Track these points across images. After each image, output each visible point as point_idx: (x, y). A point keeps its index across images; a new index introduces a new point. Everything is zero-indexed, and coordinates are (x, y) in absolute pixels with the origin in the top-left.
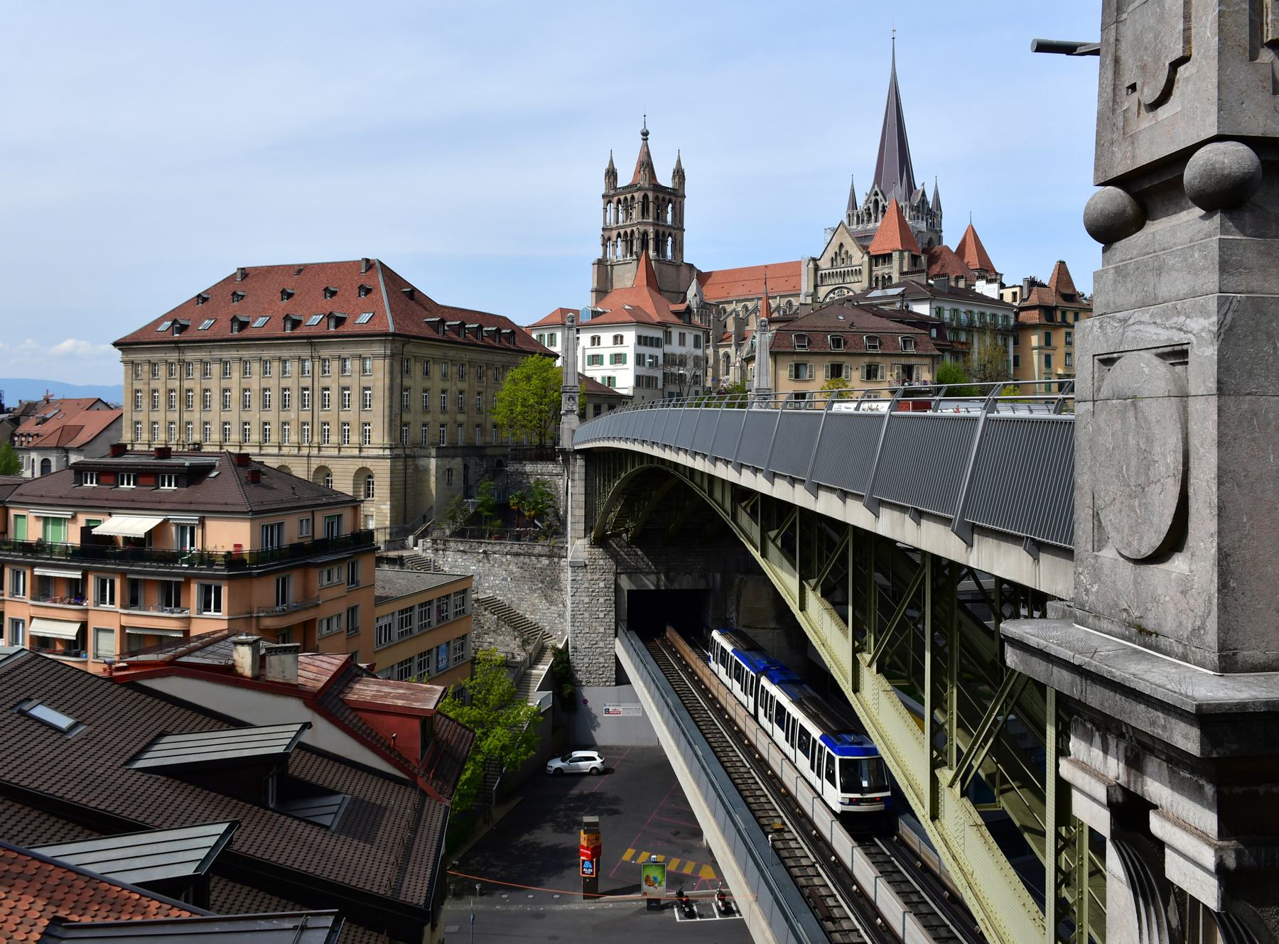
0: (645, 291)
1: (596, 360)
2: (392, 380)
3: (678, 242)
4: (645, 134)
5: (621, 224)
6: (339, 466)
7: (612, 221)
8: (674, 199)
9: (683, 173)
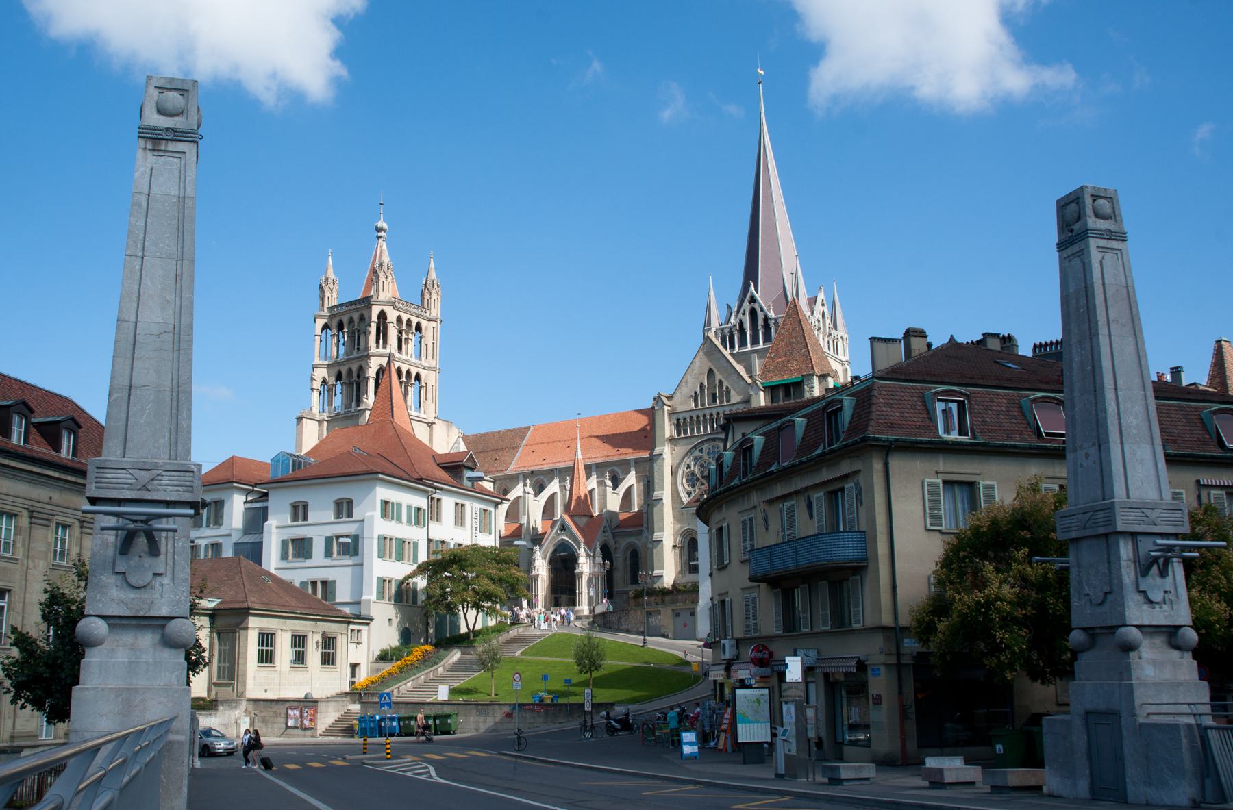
8: (424, 323)
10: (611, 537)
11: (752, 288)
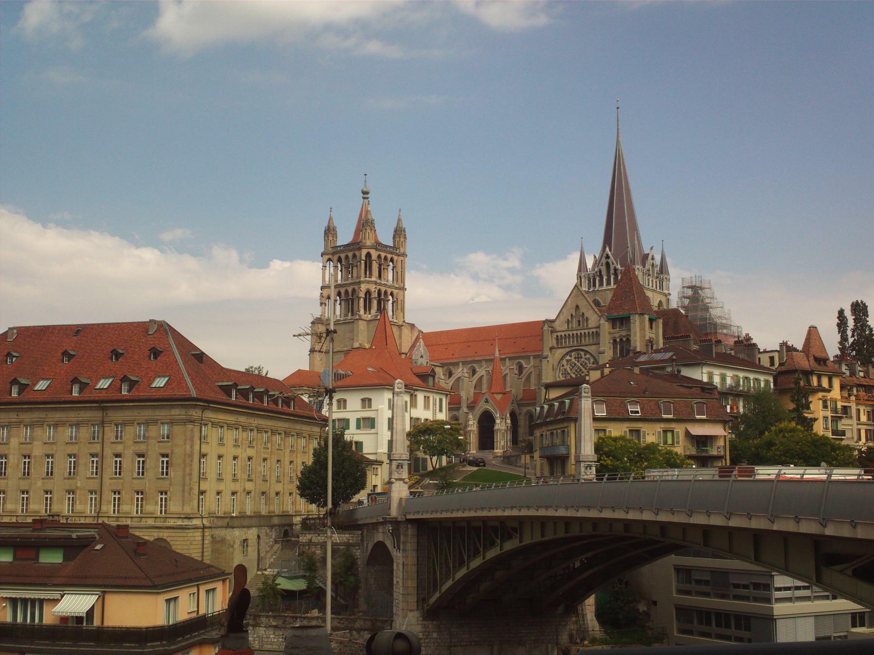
3: (399, 301)
8: (395, 258)
10: (516, 406)
11: (607, 249)
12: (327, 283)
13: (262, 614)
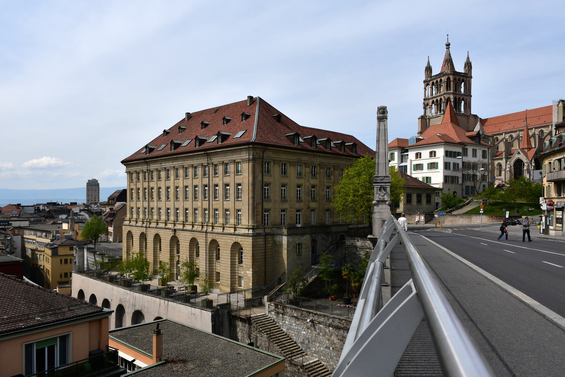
0: (450, 125)
1: (419, 167)
2: (254, 178)
3: (468, 103)
4: (448, 45)
5: (434, 95)
6: (223, 240)
7: (429, 95)
8: (465, 79)
9: (471, 64)
12: (427, 97)
13: (288, 306)
